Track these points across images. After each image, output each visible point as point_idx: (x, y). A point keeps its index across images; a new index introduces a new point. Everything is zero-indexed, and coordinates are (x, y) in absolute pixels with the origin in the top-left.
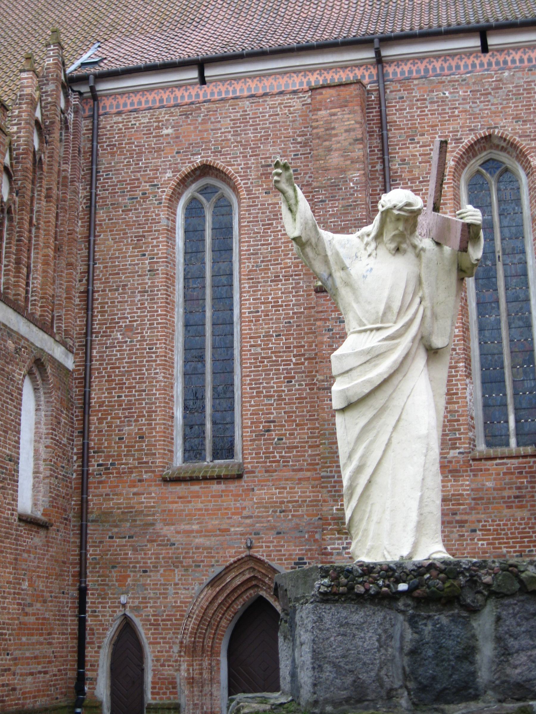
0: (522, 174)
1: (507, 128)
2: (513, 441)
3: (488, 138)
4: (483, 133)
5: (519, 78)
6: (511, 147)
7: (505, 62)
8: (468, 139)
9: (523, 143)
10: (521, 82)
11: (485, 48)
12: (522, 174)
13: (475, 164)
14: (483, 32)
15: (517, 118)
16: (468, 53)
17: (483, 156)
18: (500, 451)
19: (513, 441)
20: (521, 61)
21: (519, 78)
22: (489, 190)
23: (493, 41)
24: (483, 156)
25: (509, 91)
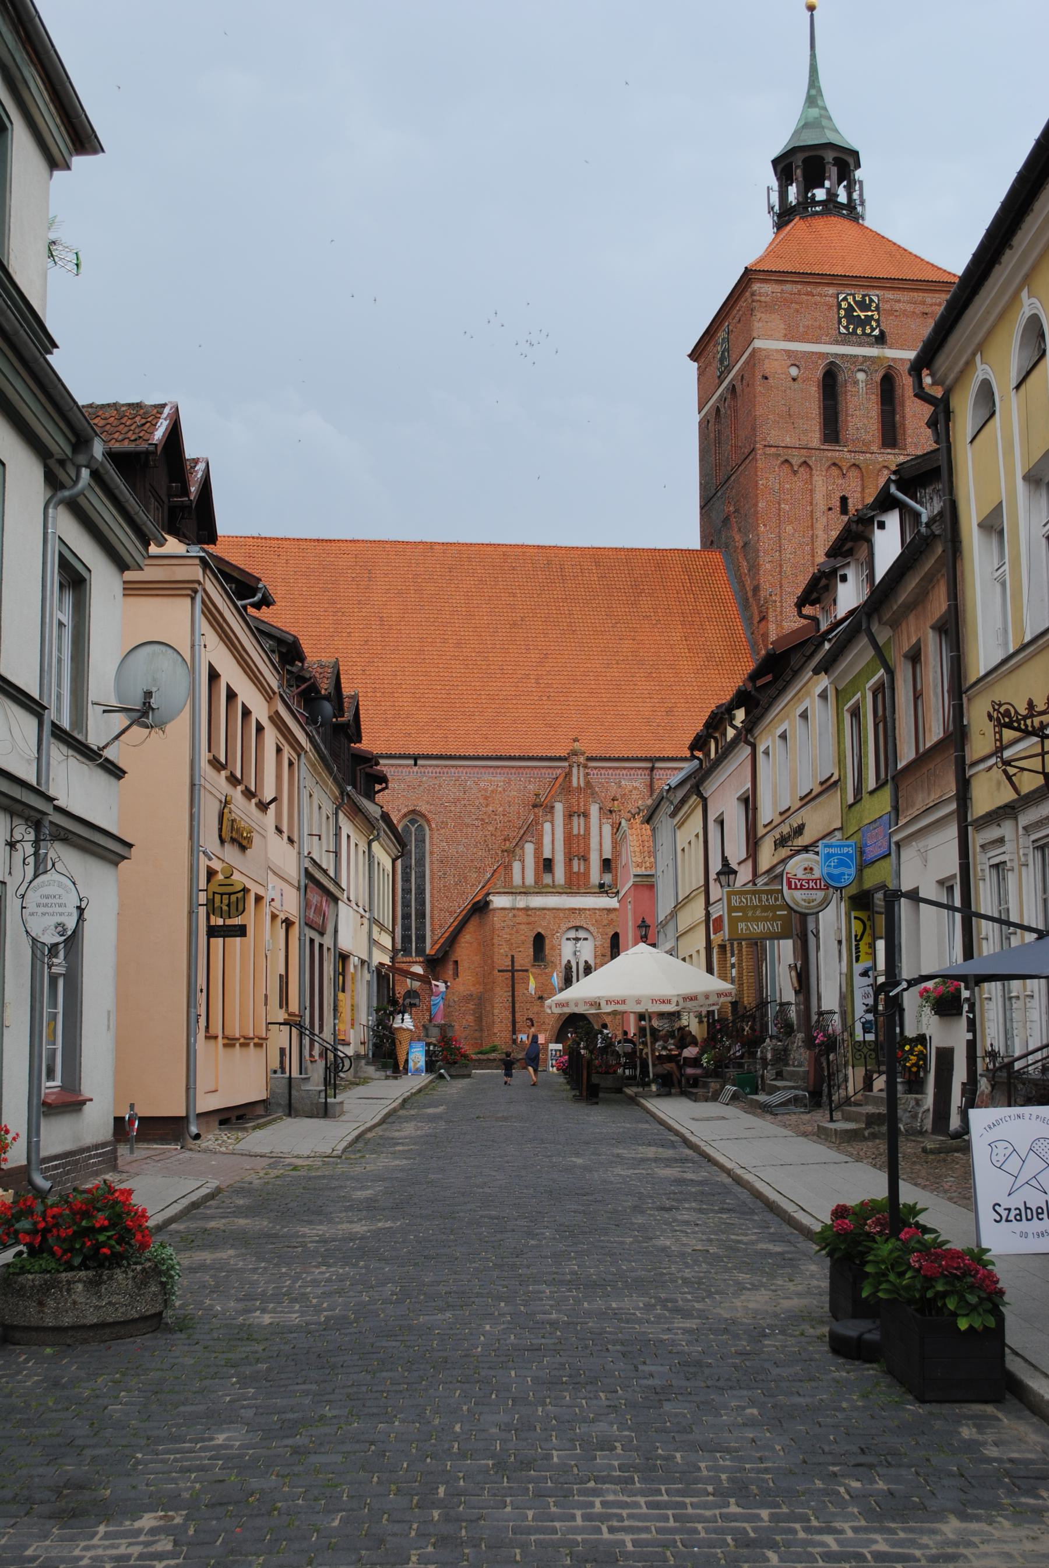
0: (427, 828)
1: (423, 808)
2: (414, 954)
3: (413, 811)
4: (411, 808)
6: (423, 816)
8: (404, 810)
9: (429, 816)
11: (416, 764)
12: (427, 828)
13: (405, 821)
14: (416, 758)
15: (428, 803)
16: (408, 766)
17: (410, 817)
18: (408, 959)
19: (414, 954)
22: (411, 834)
23: (419, 762)
24: (410, 817)
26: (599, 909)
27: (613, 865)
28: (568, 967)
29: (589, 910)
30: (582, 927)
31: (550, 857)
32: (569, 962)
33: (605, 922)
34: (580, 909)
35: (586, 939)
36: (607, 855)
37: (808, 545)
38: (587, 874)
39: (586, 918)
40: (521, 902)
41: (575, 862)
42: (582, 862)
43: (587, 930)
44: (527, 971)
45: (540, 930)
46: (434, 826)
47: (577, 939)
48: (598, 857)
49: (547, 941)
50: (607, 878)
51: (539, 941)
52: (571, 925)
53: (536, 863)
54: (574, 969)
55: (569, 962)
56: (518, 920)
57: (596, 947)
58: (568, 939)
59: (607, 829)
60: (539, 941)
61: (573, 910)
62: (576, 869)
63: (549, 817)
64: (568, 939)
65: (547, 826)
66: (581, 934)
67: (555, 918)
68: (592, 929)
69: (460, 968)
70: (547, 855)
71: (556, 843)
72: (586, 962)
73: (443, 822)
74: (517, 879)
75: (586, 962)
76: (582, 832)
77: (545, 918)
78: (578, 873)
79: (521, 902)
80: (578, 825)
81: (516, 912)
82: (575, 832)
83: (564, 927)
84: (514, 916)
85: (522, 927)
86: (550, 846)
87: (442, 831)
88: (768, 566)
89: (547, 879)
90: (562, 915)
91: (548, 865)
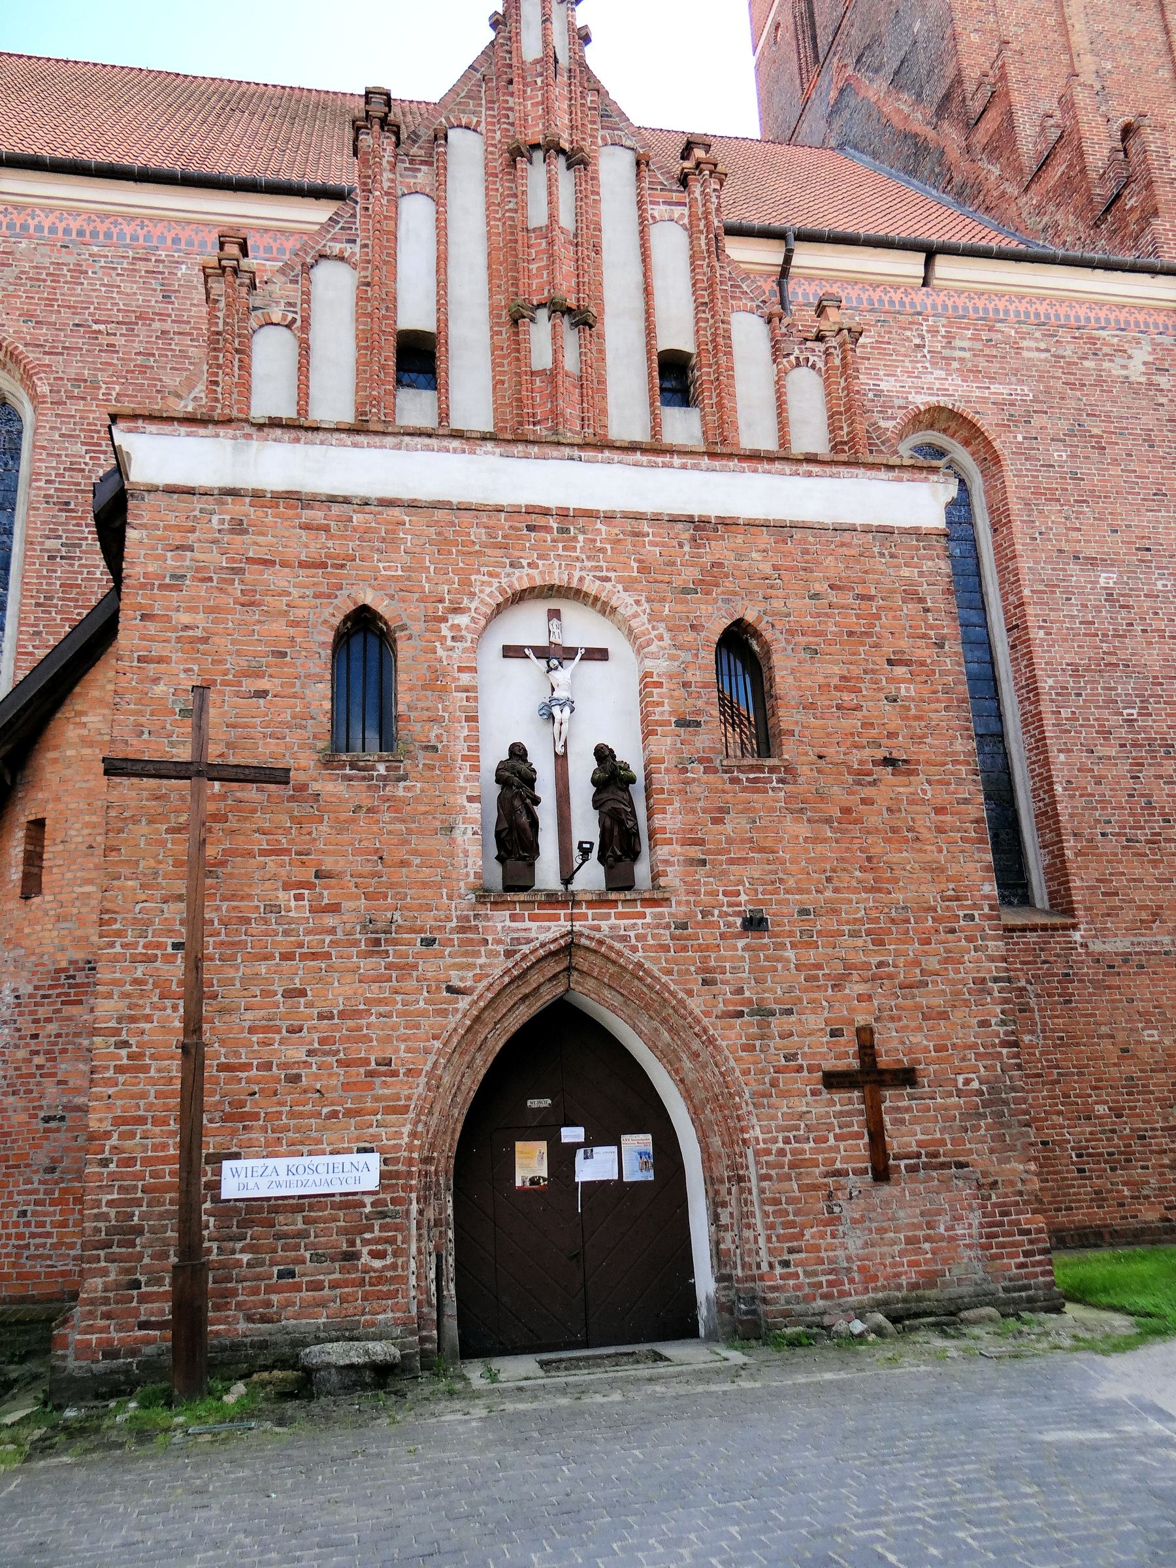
5: (43, 256)
7: (25, 227)
10: (46, 262)
15: (28, 316)
20: (53, 230)
21: (43, 256)
25: (23, 272)
26: (656, 519)
27: (702, 374)
28: (516, 776)
29: (609, 517)
30: (575, 594)
31: (427, 324)
32: (518, 752)
33: (689, 575)
34: (563, 514)
35: (598, 655)
36: (677, 334)
37: (1050, 14)
38: (591, 384)
39: (595, 552)
40: (277, 465)
41: (540, 334)
42: (571, 338)
43: (606, 609)
44: (279, 776)
45: (368, 598)
46: (43, 388)
47: (553, 655)
48: (639, 341)
49: (405, 650)
50: (683, 426)
51: (364, 640)
52: (521, 579)
53: (366, 343)
54: (545, 787)
55: (518, 752)
56: (253, 545)
57: (647, 682)
58: (511, 652)
59: (671, 244)
60: (364, 640)
61: (534, 518)
62: (541, 355)
63: (424, 176)
64: (511, 652)
65: (415, 215)
66: (580, 627)
67: (443, 544)
68: (624, 600)
69: (51, 852)
70: (415, 314)
71: (455, 276)
72: (603, 754)
73: (78, 380)
74: (271, 396)
75: (603, 754)
76: (566, 220)
77: (390, 541)
78: (552, 376)
79: (277, 465)
80: (545, 190)
81: (243, 508)
82: (537, 216)
83: (488, 593)
84: (239, 527)
85: (277, 578)
86: (429, 283)
87: (72, 408)
88: (975, 37)
89: (416, 406)
90: (478, 534)
91: (418, 358)
